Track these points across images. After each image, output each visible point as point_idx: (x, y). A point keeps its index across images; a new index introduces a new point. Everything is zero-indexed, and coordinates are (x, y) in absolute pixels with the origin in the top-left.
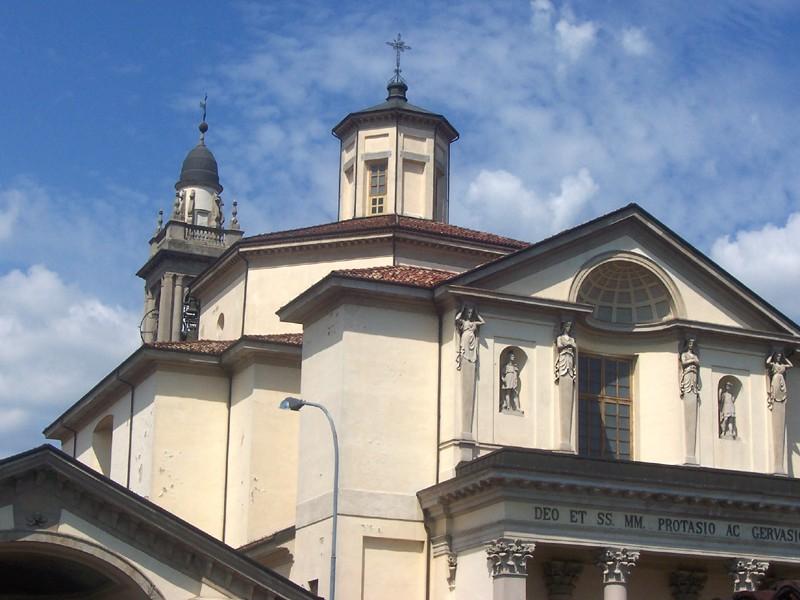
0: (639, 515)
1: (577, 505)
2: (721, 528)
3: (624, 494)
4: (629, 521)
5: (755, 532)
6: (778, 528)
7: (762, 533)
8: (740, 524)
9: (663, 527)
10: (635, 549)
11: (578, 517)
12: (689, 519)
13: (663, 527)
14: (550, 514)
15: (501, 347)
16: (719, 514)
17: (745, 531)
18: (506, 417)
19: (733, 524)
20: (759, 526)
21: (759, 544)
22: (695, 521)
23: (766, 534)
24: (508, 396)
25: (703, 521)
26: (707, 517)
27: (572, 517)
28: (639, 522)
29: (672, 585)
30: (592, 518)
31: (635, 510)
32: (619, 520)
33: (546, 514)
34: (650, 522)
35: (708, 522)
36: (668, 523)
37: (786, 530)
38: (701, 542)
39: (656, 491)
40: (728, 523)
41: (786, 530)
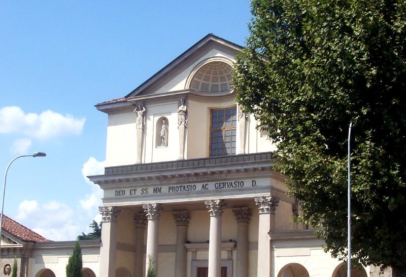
0: (159, 187)
1: (132, 187)
2: (199, 186)
3: (150, 178)
4: (155, 191)
5: (217, 185)
6: (229, 182)
7: (220, 185)
8: (209, 183)
9: (171, 191)
10: (217, 199)
11: (133, 192)
12: (183, 185)
13: (171, 191)
14: (121, 193)
15: (157, 118)
16: (195, 180)
17: (211, 186)
18: (162, 149)
19: (205, 184)
20: (219, 182)
21: (218, 191)
22: (186, 185)
23: (222, 186)
24: (161, 140)
25: (190, 184)
26: (190, 182)
27: (131, 192)
28: (160, 191)
29: (135, 219)
30: (139, 192)
31: (156, 185)
32: (151, 190)
33: (120, 193)
34: (165, 189)
35: (193, 185)
36: (173, 188)
37: (233, 182)
38: (188, 195)
39: (158, 175)
40: (202, 184)
41: (233, 182)
